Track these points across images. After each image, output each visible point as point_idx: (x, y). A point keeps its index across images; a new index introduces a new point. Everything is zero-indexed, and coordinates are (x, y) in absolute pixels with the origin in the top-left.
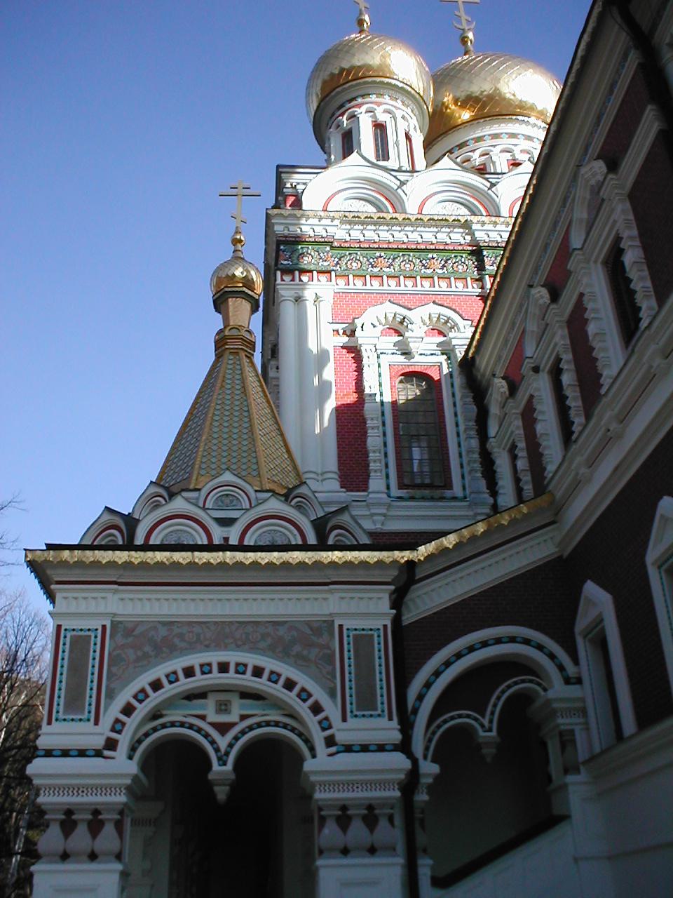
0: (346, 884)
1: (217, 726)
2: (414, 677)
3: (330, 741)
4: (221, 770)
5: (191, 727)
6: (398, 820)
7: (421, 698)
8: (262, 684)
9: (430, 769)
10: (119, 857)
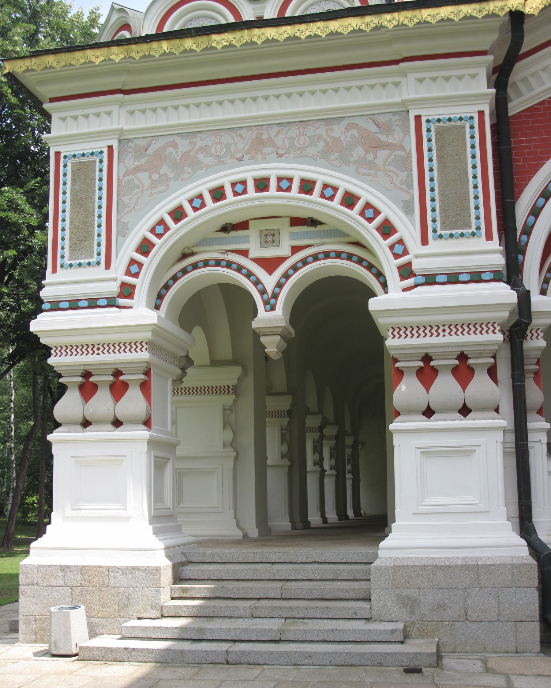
0: (428, 453)
1: (261, 262)
2: (526, 185)
3: (406, 271)
4: (272, 318)
5: (229, 265)
6: (504, 372)
8: (313, 204)
10: (147, 423)
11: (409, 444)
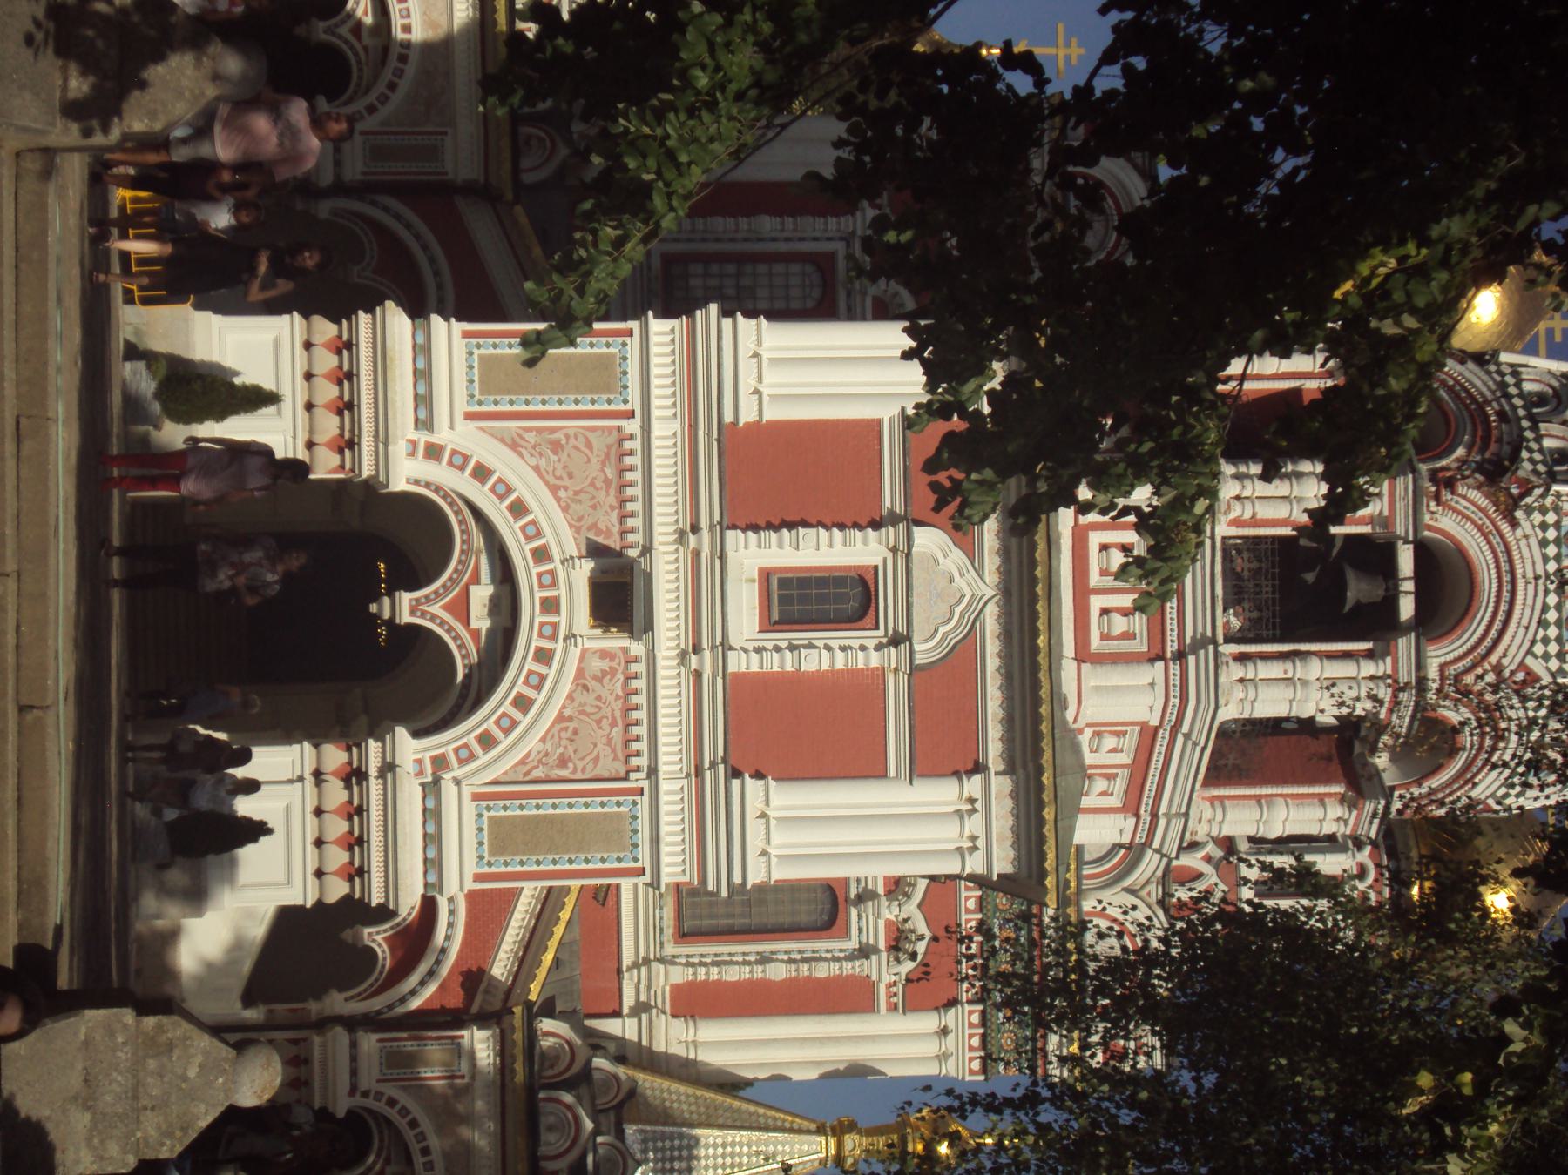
7: (386, 209)
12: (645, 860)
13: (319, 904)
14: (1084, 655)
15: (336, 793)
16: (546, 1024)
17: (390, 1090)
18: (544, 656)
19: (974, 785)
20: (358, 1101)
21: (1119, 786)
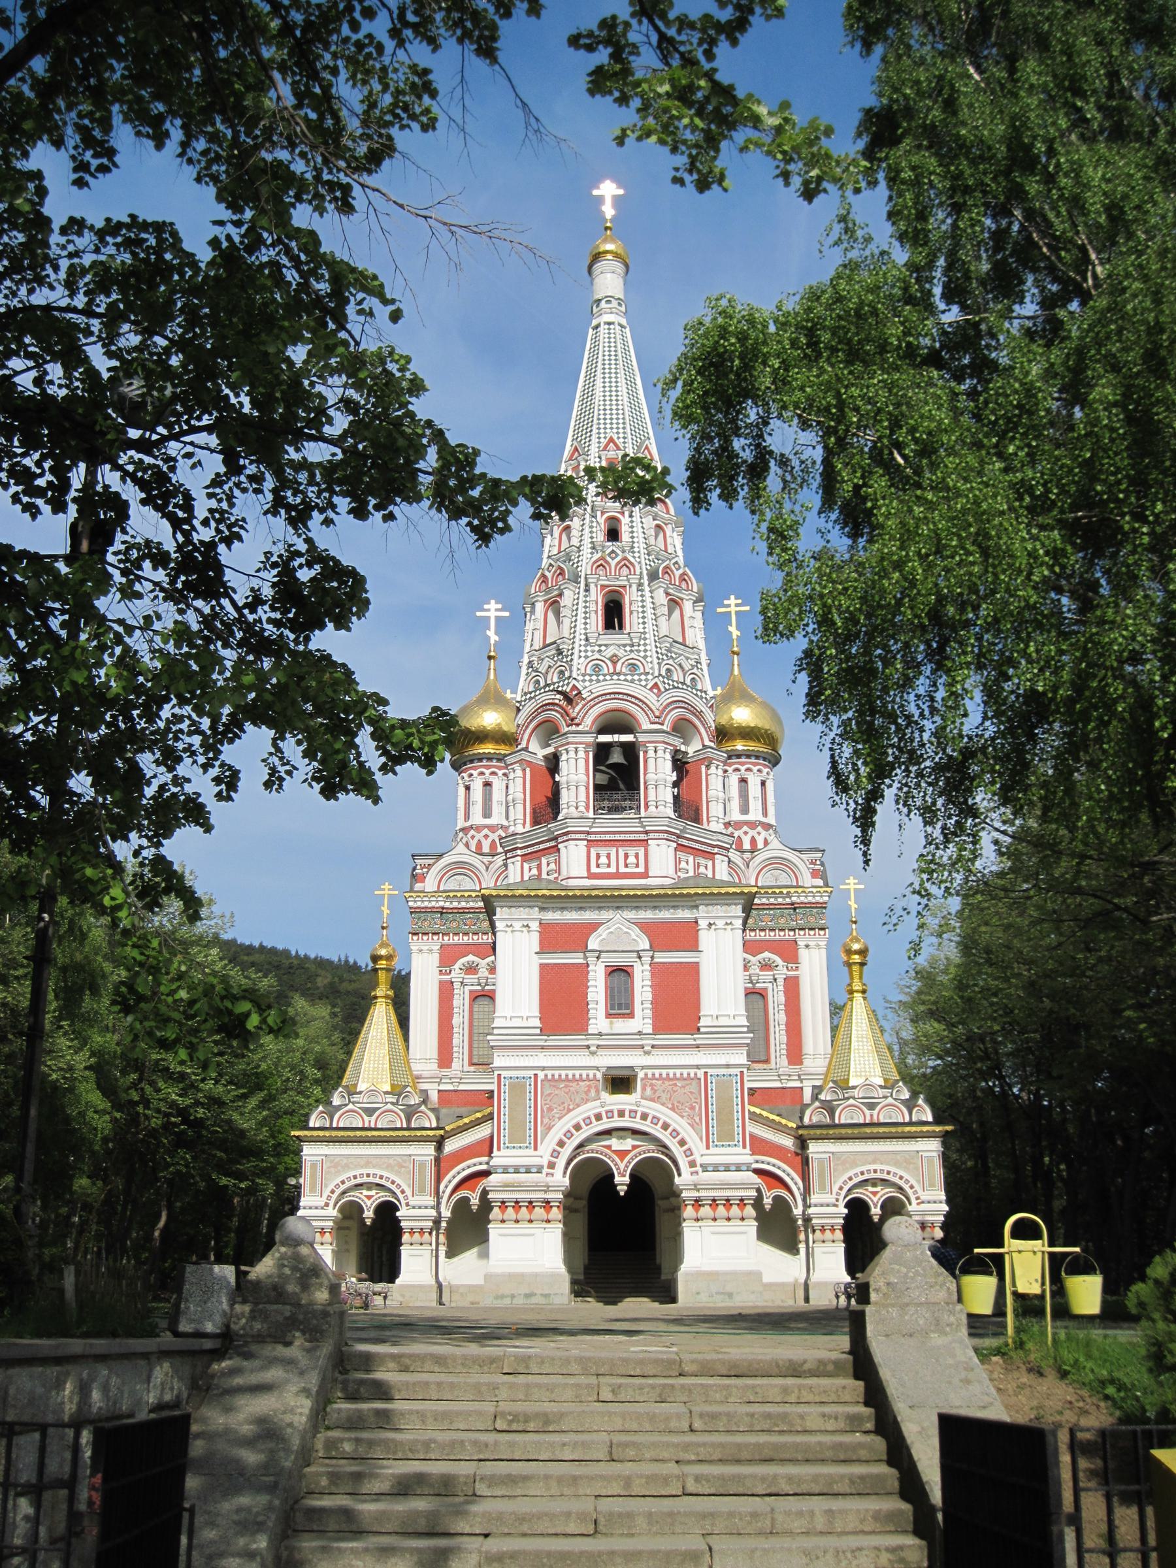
4: (369, 1214)
8: (382, 1182)
9: (446, 1213)
11: (406, 1252)
12: (737, 1071)
13: (756, 1219)
14: (645, 875)
15: (706, 1211)
16: (806, 1121)
17: (835, 1189)
18: (644, 1117)
19: (703, 924)
20: (842, 1204)
21: (702, 861)
